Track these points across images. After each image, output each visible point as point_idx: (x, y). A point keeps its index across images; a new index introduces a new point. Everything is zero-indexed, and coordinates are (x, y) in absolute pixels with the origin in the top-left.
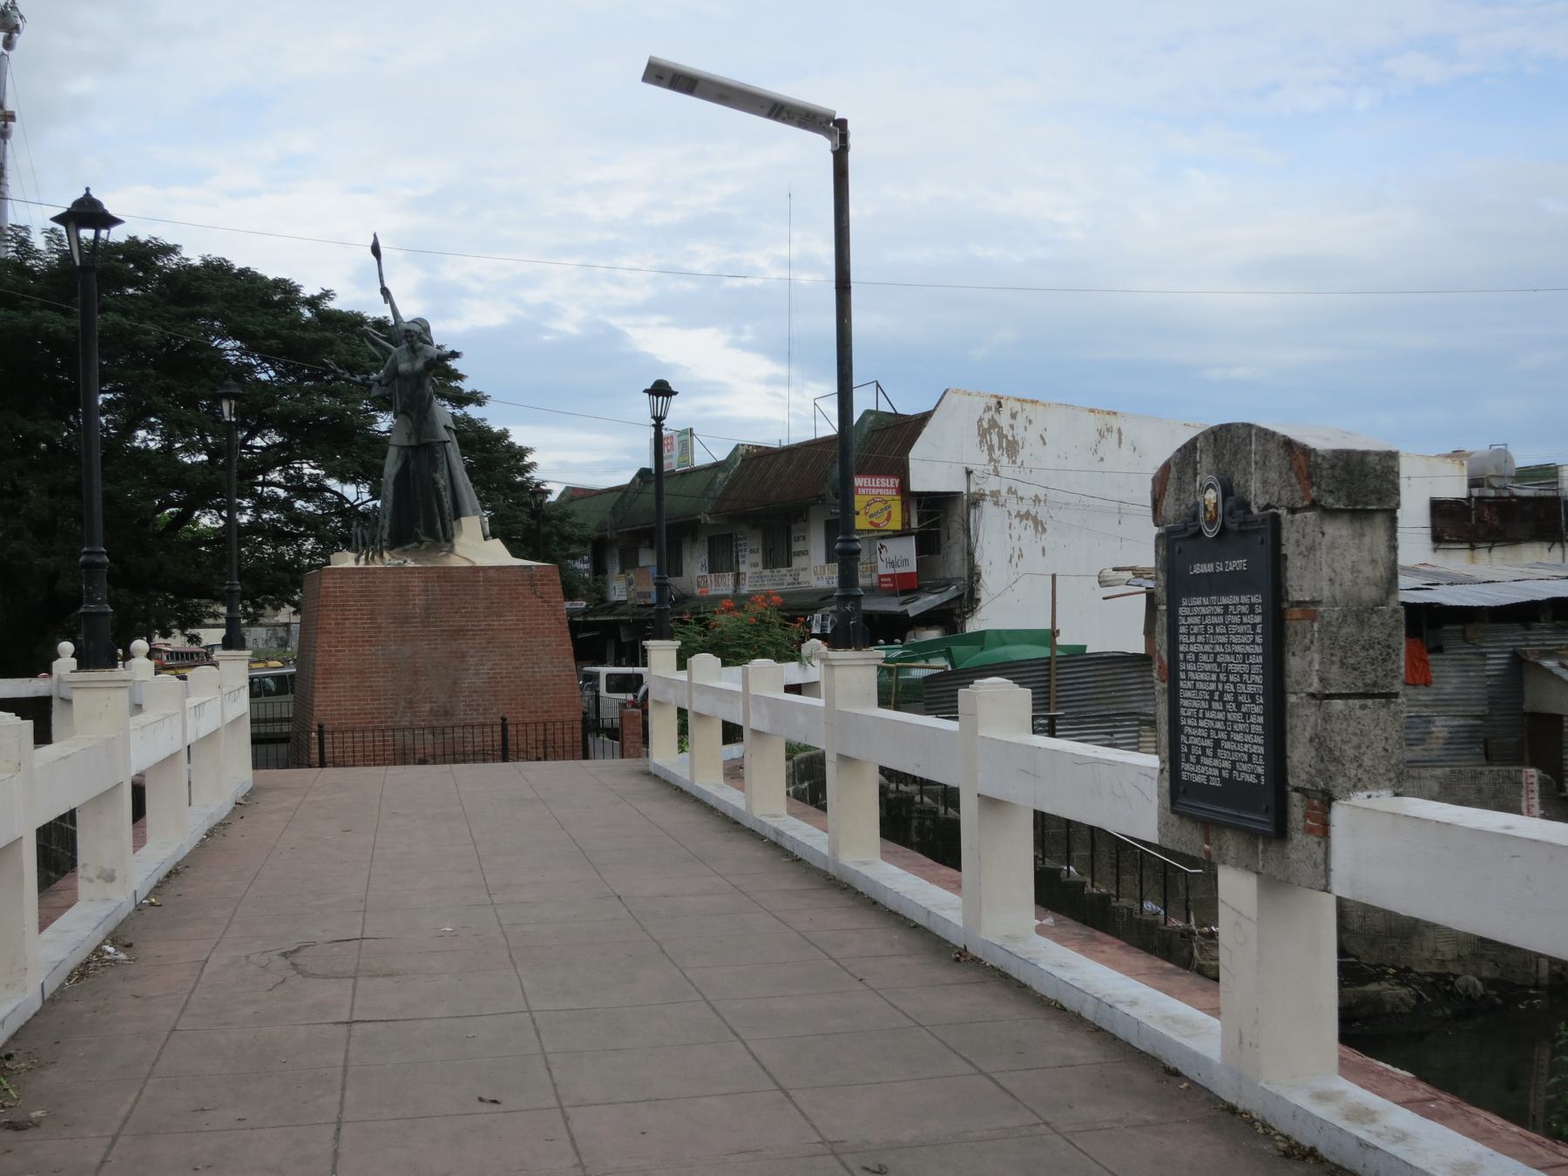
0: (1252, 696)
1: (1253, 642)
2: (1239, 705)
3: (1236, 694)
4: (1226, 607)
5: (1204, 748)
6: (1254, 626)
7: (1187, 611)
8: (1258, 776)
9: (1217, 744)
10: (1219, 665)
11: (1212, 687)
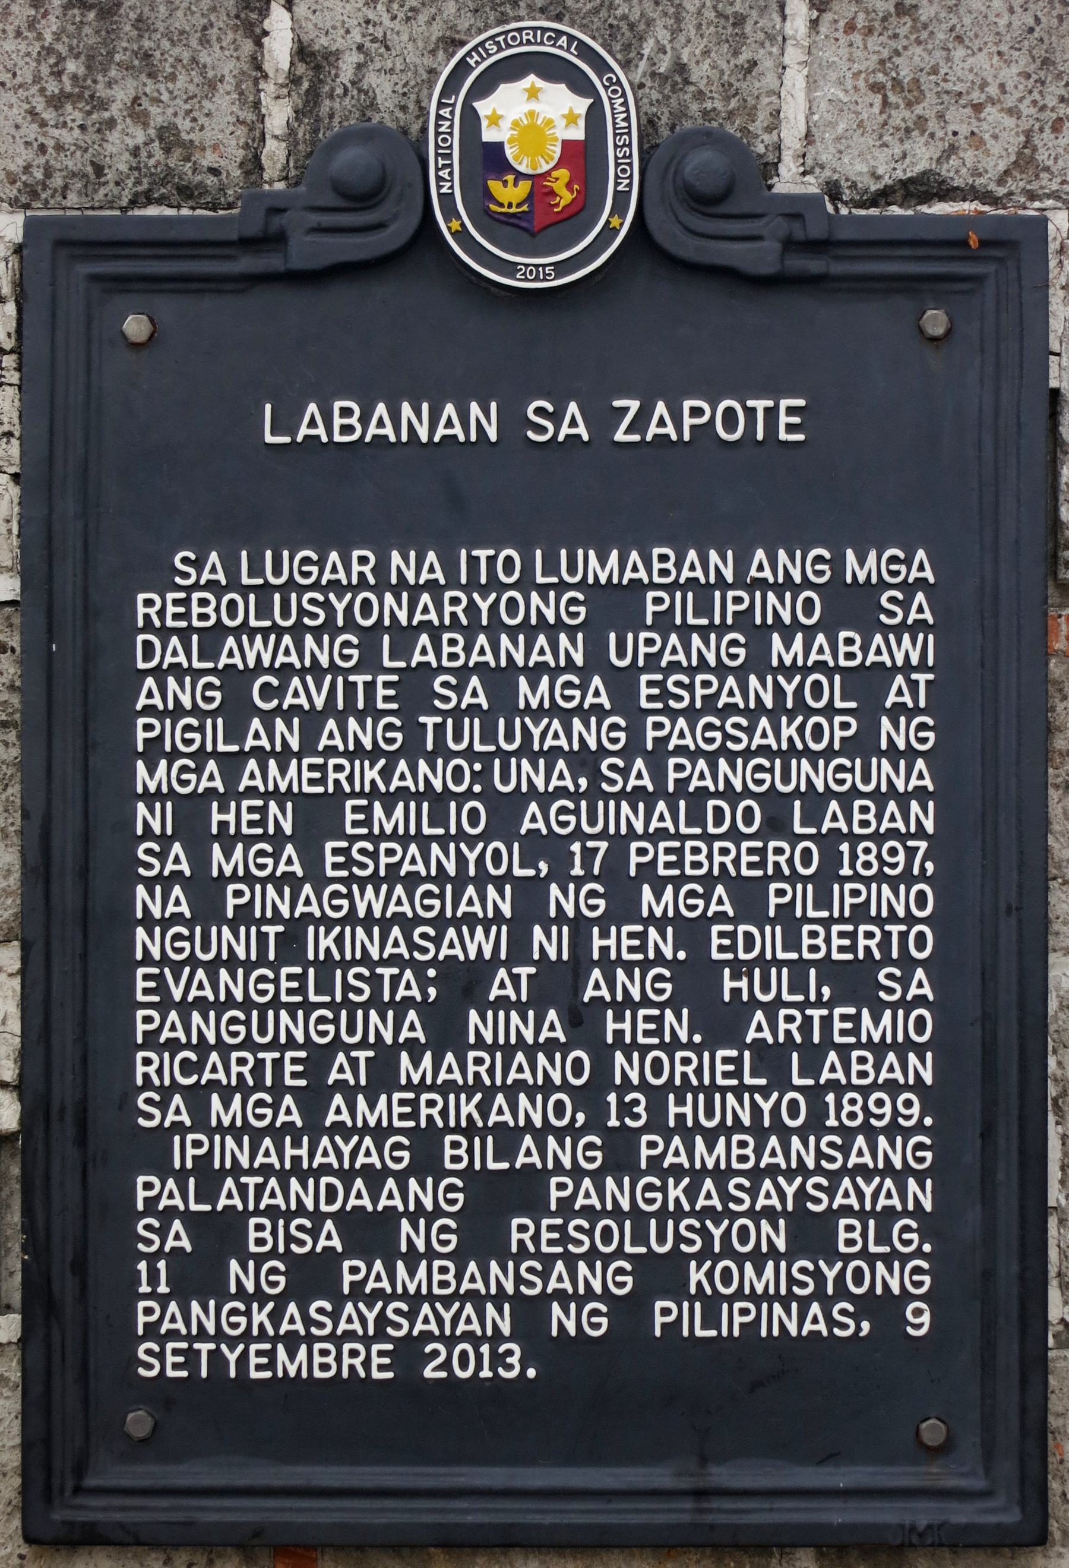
0: (853, 981)
1: (865, 745)
2: (720, 1023)
3: (695, 981)
4: (614, 606)
5: (370, 1234)
6: (867, 684)
7: (207, 611)
8: (883, 1308)
9: (496, 1203)
10: (536, 846)
11: (480, 943)
